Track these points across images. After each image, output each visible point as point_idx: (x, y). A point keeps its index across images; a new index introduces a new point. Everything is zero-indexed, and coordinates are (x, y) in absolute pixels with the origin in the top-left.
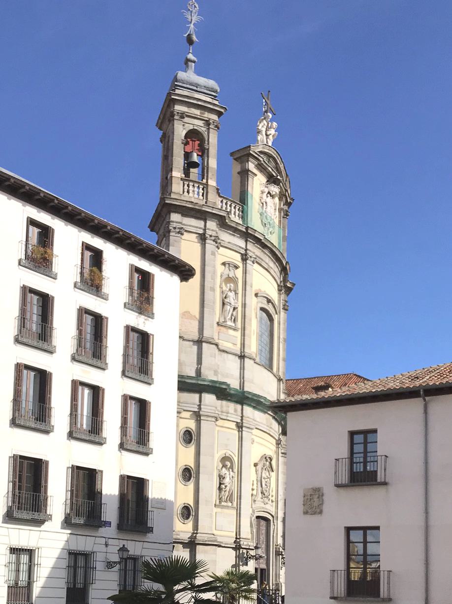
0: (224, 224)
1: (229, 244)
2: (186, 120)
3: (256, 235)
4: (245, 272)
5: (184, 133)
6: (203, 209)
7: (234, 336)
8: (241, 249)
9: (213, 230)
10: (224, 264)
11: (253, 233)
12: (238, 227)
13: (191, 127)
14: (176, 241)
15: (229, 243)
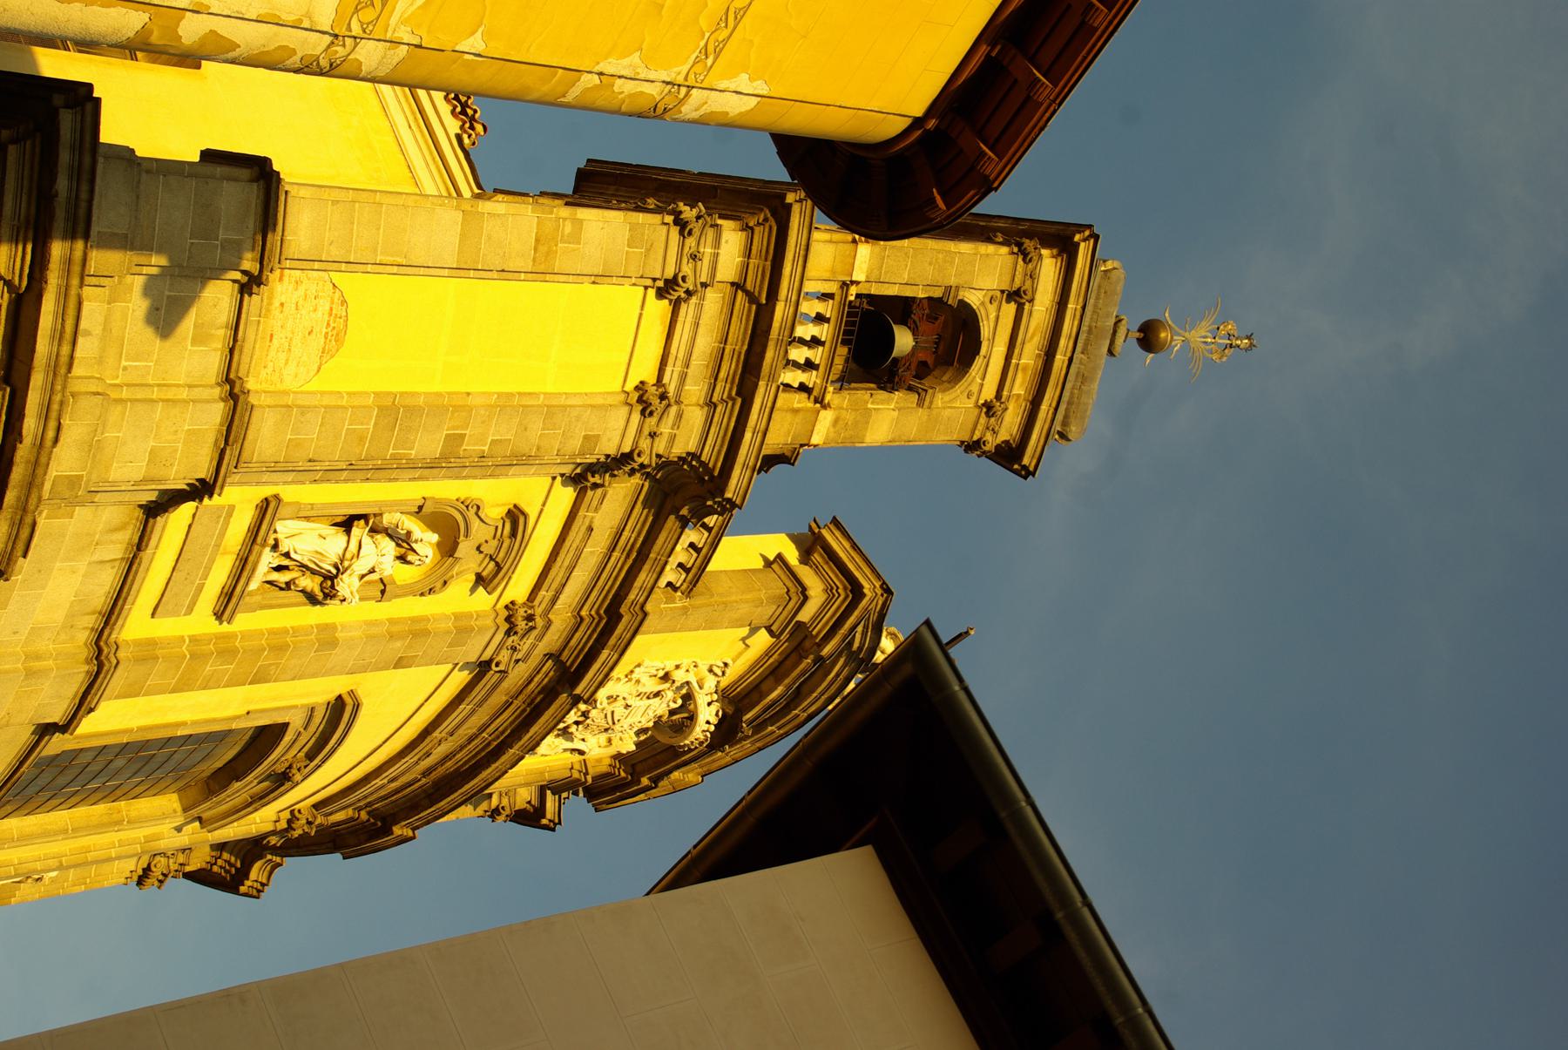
0: (666, 495)
1: (584, 528)
2: (1010, 309)
3: (605, 653)
4: (463, 627)
5: (973, 299)
6: (762, 384)
7: (200, 588)
8: (551, 593)
9: (673, 438)
10: (515, 517)
11: (612, 641)
12: (647, 567)
13: (985, 331)
14: (648, 250)
15: (590, 529)
